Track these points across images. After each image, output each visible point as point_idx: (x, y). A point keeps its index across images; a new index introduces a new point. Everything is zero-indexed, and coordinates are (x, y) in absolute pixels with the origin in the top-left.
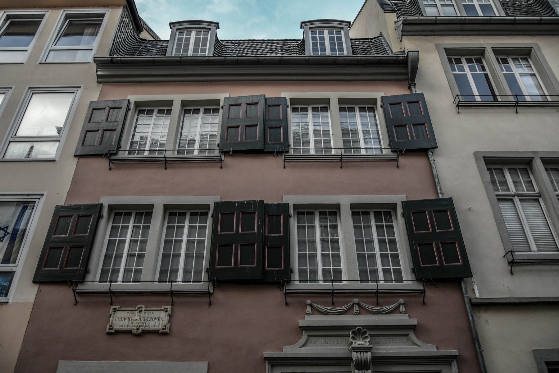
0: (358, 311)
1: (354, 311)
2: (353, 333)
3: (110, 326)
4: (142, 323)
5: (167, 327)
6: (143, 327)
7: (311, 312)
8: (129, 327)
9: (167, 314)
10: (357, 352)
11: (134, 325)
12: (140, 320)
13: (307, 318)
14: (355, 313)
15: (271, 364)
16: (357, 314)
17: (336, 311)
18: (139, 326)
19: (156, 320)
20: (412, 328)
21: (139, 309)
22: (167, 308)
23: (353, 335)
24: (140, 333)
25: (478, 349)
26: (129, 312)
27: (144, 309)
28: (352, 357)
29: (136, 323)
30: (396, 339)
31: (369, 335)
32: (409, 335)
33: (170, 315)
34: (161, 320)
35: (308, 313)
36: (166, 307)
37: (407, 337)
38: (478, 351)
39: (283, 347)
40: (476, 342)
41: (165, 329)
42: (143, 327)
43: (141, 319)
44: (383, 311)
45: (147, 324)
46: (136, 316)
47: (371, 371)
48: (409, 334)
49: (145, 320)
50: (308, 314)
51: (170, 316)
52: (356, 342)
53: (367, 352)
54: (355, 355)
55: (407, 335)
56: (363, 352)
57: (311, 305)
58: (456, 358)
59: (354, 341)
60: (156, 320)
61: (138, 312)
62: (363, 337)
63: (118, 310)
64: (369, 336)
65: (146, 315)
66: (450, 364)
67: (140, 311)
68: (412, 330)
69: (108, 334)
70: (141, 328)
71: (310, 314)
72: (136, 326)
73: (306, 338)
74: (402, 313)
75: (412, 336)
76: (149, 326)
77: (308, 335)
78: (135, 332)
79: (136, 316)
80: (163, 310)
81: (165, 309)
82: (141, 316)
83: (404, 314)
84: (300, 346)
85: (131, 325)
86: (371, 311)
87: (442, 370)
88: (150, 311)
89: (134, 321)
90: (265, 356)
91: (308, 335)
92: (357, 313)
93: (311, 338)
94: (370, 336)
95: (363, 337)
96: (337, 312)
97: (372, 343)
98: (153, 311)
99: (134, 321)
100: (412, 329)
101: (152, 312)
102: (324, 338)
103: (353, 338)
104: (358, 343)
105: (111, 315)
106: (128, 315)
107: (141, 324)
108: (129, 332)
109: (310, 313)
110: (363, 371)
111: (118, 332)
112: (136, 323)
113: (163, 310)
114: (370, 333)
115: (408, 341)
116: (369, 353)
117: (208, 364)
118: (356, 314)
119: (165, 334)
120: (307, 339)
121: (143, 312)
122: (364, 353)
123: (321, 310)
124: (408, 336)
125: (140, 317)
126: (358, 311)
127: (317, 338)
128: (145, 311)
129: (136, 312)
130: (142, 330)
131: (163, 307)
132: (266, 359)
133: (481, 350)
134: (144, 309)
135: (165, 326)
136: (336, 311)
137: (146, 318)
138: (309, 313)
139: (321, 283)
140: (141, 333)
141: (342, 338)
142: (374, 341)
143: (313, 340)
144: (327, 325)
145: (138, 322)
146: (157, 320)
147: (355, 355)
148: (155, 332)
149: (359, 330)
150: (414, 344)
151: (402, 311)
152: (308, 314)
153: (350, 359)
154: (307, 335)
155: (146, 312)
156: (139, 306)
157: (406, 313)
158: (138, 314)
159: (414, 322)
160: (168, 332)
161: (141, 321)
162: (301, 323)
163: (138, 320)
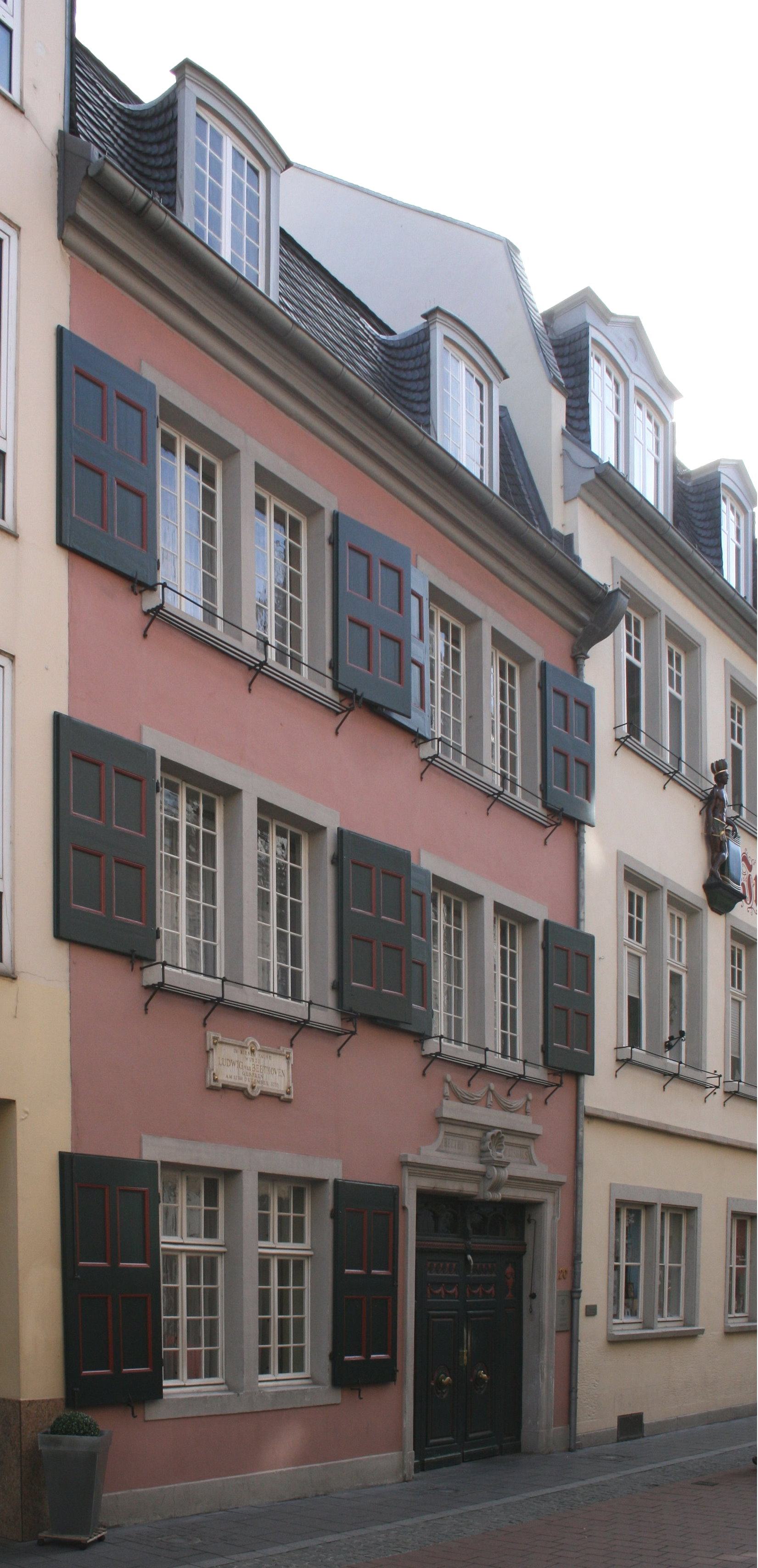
1: (489, 1103)
3: (214, 1074)
8: (241, 1081)
11: (247, 1077)
18: (253, 1080)
26: (237, 1048)
27: (259, 1047)
46: (249, 1061)
57: (449, 1083)
61: (248, 1051)
63: (221, 1043)
65: (262, 1060)
69: (212, 1089)
70: (257, 1085)
77: (447, 1133)
78: (250, 1090)
79: (247, 1059)
85: (243, 1077)
86: (502, 1105)
88: (266, 1054)
105: (212, 1050)
106: (236, 1054)
108: (242, 1091)
111: (225, 1087)
113: (284, 1055)
119: (289, 1101)
121: (257, 1053)
123: (459, 1093)
130: (261, 1091)
131: (282, 1048)
139: (465, 1047)
148: (277, 1097)
150: (532, 1163)
159: (537, 1129)
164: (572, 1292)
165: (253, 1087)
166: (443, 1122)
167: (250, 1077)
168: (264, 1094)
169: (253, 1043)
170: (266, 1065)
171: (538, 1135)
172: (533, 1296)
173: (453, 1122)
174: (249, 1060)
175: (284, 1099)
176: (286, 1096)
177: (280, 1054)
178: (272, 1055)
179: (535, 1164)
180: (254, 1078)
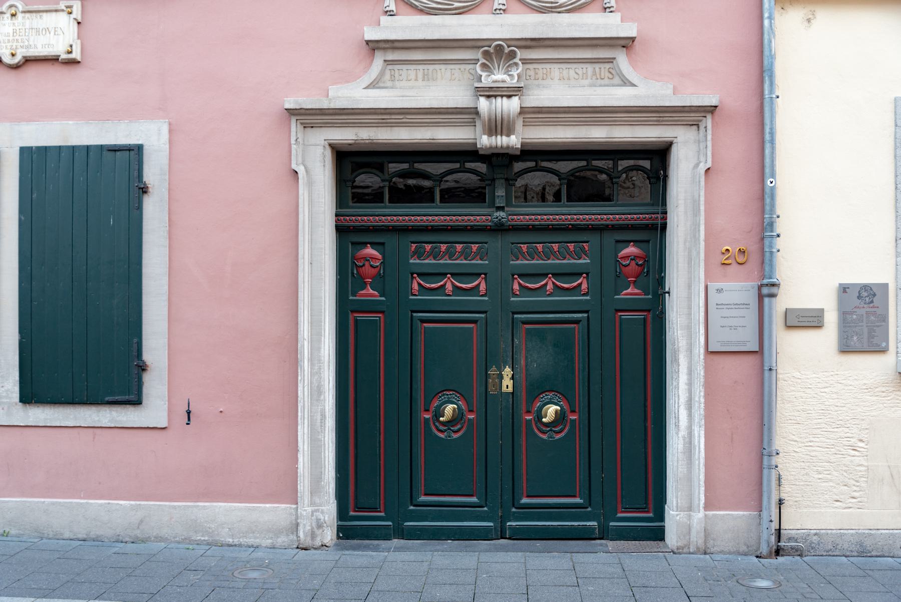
0: (504, 5)
2: (486, 54)
4: (20, 41)
5: (74, 47)
6: (24, 50)
7: (394, 9)
9: (72, 20)
10: (488, 97)
11: (4, 45)
12: (15, 34)
13: (385, 20)
14: (495, 10)
15: (302, 124)
16: (502, 12)
17: (453, 5)
18: (14, 47)
19: (50, 33)
20: (626, 44)
21: (10, 10)
22: (70, 7)
23: (484, 61)
24: (19, 62)
25: (766, 92)
28: (477, 108)
29: (9, 41)
30: (585, 69)
31: (520, 60)
32: (614, 62)
33: (80, 21)
34: (62, 34)
35: (387, 12)
36: (68, 4)
37: (608, 66)
38: (767, 96)
39: (330, 87)
40: (767, 78)
41: (70, 52)
42: (24, 50)
43: (18, 32)
44: (561, 6)
45: (31, 43)
47: (516, 138)
48: (615, 58)
49: (27, 34)
50: (388, 13)
51: (79, 23)
52: (490, 75)
53: (509, 97)
54: (483, 104)
55: (611, 60)
56: (502, 96)
58: (712, 112)
59: (484, 74)
60: (50, 33)
61: (8, 15)
62: (507, 65)
64: (520, 63)
65: (28, 22)
66: (698, 125)
67: (13, 15)
68: (625, 49)
71: (392, 13)
72: (9, 47)
73: (380, 68)
74: (608, 10)
75: (622, 60)
76: (36, 47)
77: (385, 61)
79: (4, 25)
80: (63, 10)
81: (67, 7)
82: (16, 25)
83: (611, 12)
84: (365, 87)
86: (535, 6)
87: (676, 137)
88: (34, 14)
89: (4, 38)
90: (287, 106)
91: (385, 61)
92: (500, 9)
93: (390, 67)
94: (522, 63)
95: (507, 65)
96: (456, 9)
97: (528, 78)
98: (41, 14)
99: (4, 38)
100: (624, 47)
101: (38, 15)
102: (421, 67)
103: (484, 66)
104: (494, 77)
107: (19, 44)
109: (393, 11)
110: (499, 137)
112: (9, 41)
113: (63, 10)
114: (524, 57)
115: (611, 76)
116: (515, 100)
117: (170, 124)
118: (498, 12)
119: (73, 62)
120: (382, 68)
121: (20, 16)
122: (505, 99)
124: (612, 62)
125: (14, 28)
126: (504, 5)
127: (404, 67)
128: (23, 15)
129: (5, 16)
132: (291, 112)
133: (774, 96)
134: (21, 8)
135: (71, 46)
136: (453, 5)
137: (27, 30)
138: (390, 11)
140: (21, 63)
141: (463, 67)
142: (532, 78)
143: (397, 71)
144: (426, 39)
145: (11, 38)
146: (52, 33)
147: (483, 104)
149: (499, 49)
150: (626, 83)
151: (608, 5)
152: (389, 13)
153: (475, 112)
154: (383, 59)
155: (28, 15)
156: (8, 4)
157: (618, 10)
158: (9, 21)
160: (79, 60)
161: (17, 37)
162: (372, 34)
163: (11, 35)
164: (760, 287)
165: (13, 55)
166: (379, 48)
167: (9, 44)
168: (28, 61)
169: (11, 6)
170: (33, 27)
171: (633, 39)
172: (669, 293)
173: (397, 45)
174: (7, 25)
175: (62, 59)
176: (64, 56)
177: (56, 11)
178: (44, 14)
179: (634, 85)
180: (15, 44)
